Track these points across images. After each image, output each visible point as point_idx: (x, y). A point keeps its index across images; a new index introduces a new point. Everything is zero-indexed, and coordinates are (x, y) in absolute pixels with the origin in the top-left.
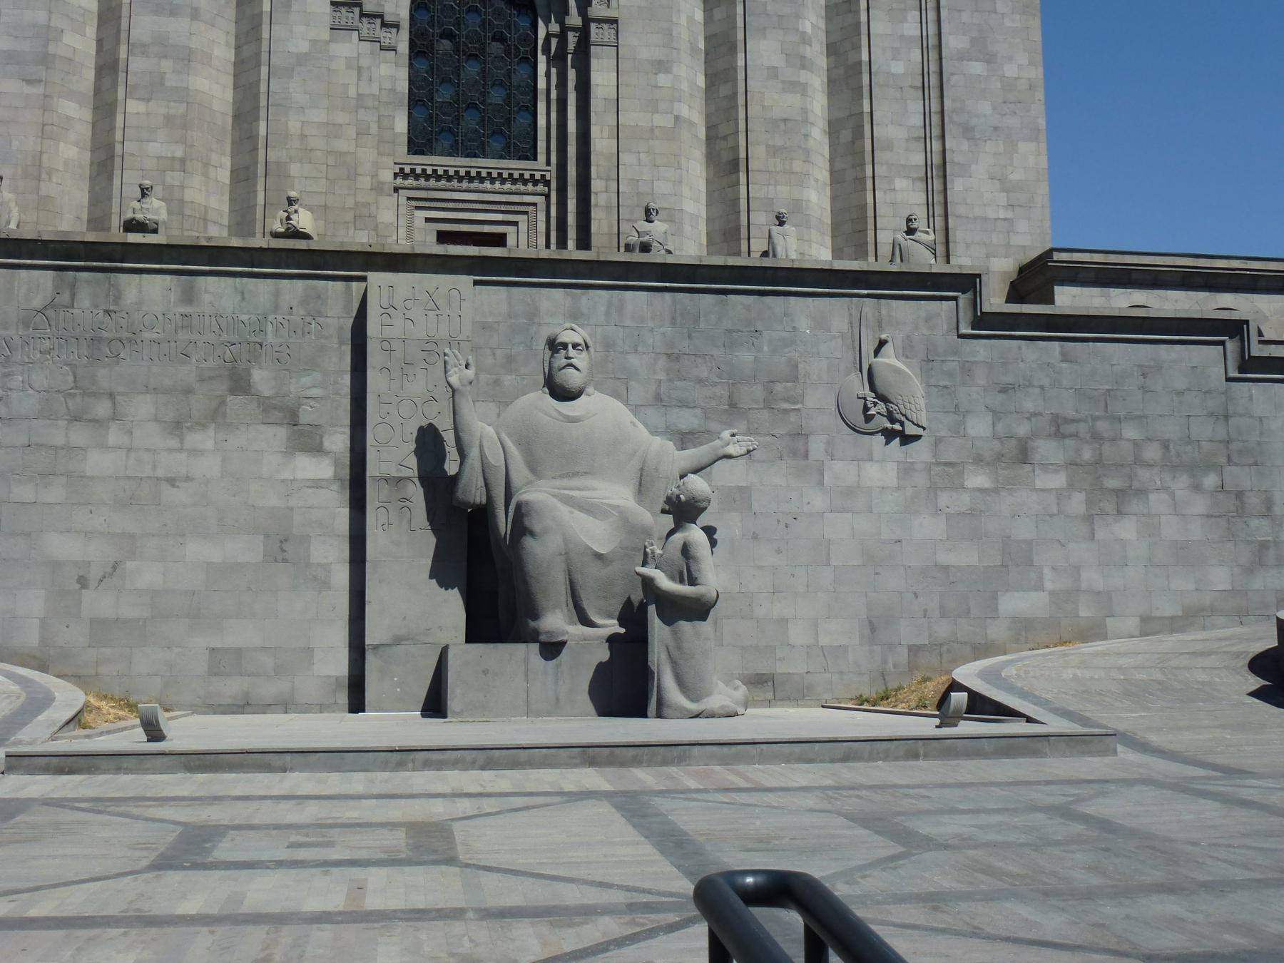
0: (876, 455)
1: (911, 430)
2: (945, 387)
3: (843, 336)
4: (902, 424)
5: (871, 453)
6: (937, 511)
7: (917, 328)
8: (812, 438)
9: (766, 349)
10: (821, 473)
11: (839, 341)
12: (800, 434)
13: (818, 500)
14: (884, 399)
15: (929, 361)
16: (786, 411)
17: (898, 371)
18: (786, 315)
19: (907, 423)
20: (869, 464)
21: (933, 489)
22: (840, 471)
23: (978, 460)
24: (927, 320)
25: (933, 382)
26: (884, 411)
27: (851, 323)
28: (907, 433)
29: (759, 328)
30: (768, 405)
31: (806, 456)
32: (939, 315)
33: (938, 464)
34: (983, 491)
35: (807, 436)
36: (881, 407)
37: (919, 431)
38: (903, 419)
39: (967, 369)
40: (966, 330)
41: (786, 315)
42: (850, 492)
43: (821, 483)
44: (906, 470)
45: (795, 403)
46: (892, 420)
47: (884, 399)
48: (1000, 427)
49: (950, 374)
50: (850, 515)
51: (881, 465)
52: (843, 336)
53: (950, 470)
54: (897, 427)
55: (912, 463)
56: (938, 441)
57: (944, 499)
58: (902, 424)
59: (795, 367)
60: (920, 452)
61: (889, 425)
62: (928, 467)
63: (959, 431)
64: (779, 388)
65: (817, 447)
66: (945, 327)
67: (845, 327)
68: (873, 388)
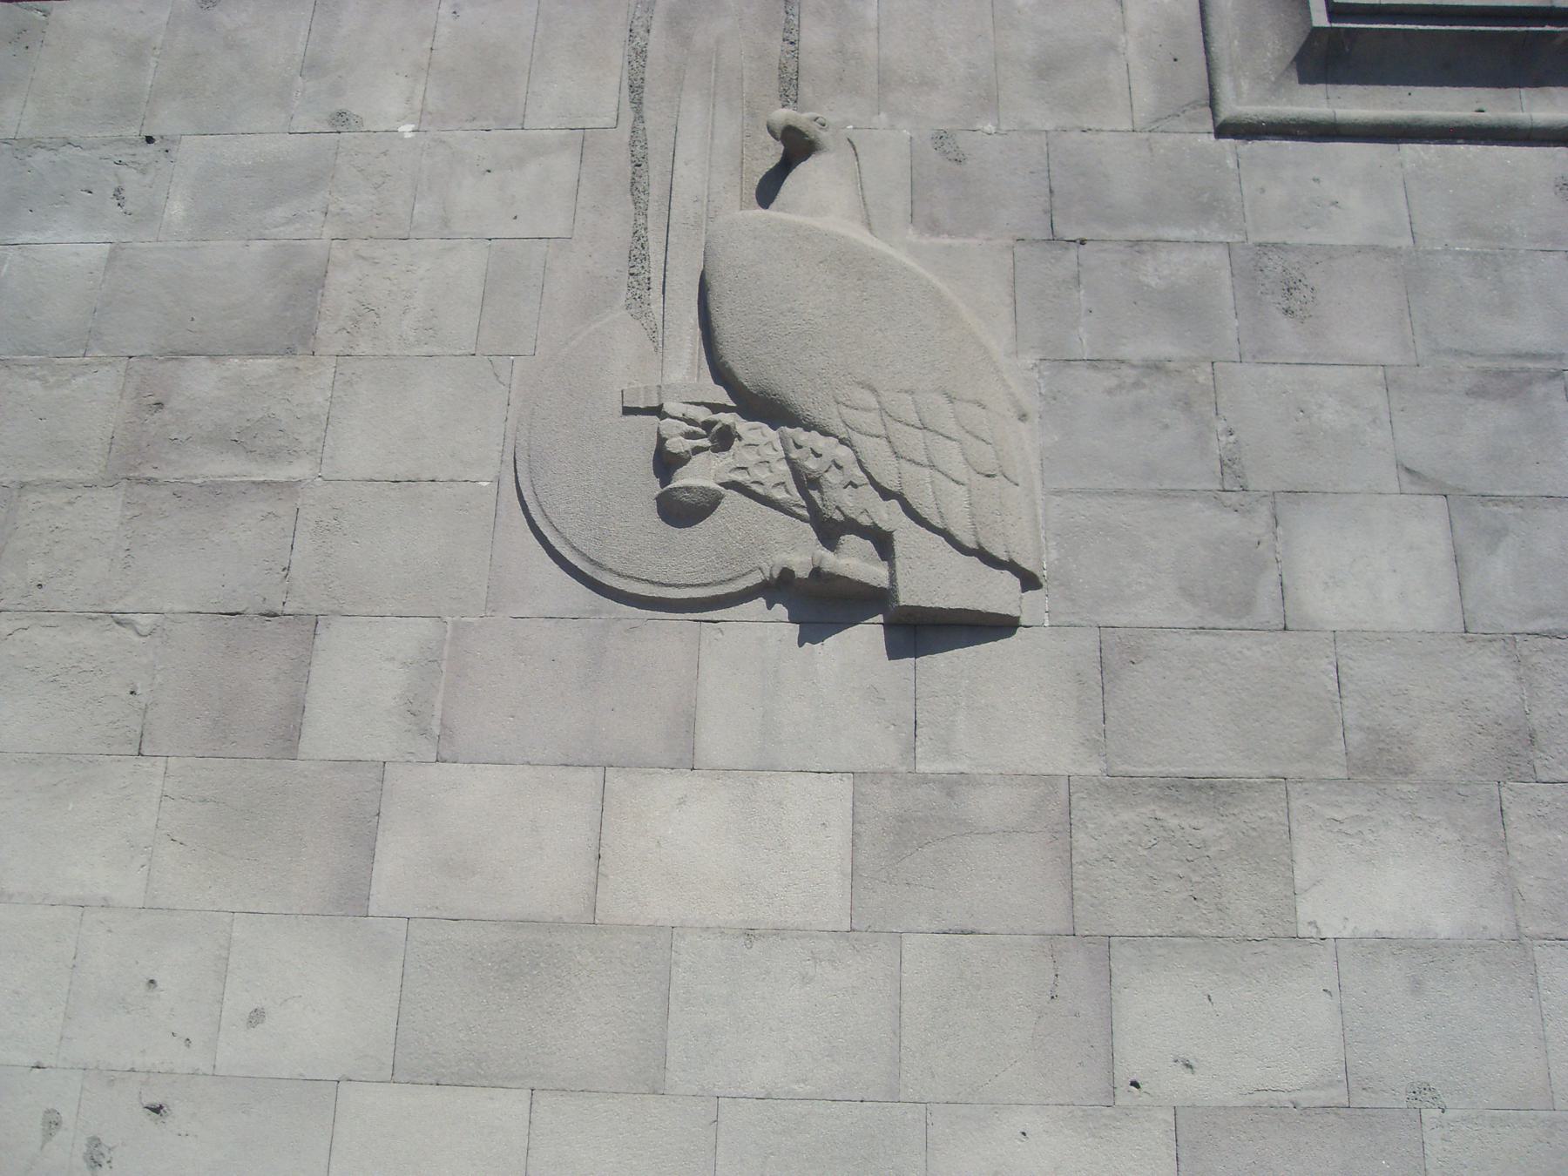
0: (719, 738)
1: (932, 578)
2: (1156, 367)
3: (583, 140)
4: (883, 543)
5: (687, 724)
6: (1113, 1093)
7: (989, 101)
8: (324, 637)
9: (176, 209)
10: (363, 836)
11: (564, 165)
12: (282, 623)
13: (318, 1002)
14: (770, 409)
15: (1054, 239)
16: (218, 492)
17: (849, 264)
18: (311, 67)
19: (907, 535)
20: (675, 784)
21: (1088, 950)
22: (492, 829)
23: (1380, 765)
24: (1047, 68)
25: (1083, 342)
26: (774, 477)
27: (636, 90)
28: (915, 591)
29: (165, 121)
30: (131, 469)
31: (287, 737)
32: (1110, 47)
33: (1121, 787)
34: (1422, 954)
35: (312, 624)
36: (760, 449)
37: (997, 593)
38: (888, 515)
39: (1280, 282)
40: (1239, 104)
41: (311, 67)
42: (527, 954)
43: (351, 898)
44: (908, 827)
45: (272, 455)
46: (830, 531)
47: (770, 409)
48: (1496, 570)
49: (1180, 307)
50: (509, 1105)
51: (753, 792)
52: (583, 140)
53: (1209, 827)
54: (855, 561)
55: (952, 785)
56: (1114, 657)
57: (1162, 1015)
58: (883, 543)
59: (305, 286)
60: (1004, 712)
61: (799, 551)
62: (1057, 810)
63: (1245, 595)
64: (202, 383)
65: (357, 686)
66: (1145, 97)
67: (604, 100)
68: (721, 374)
